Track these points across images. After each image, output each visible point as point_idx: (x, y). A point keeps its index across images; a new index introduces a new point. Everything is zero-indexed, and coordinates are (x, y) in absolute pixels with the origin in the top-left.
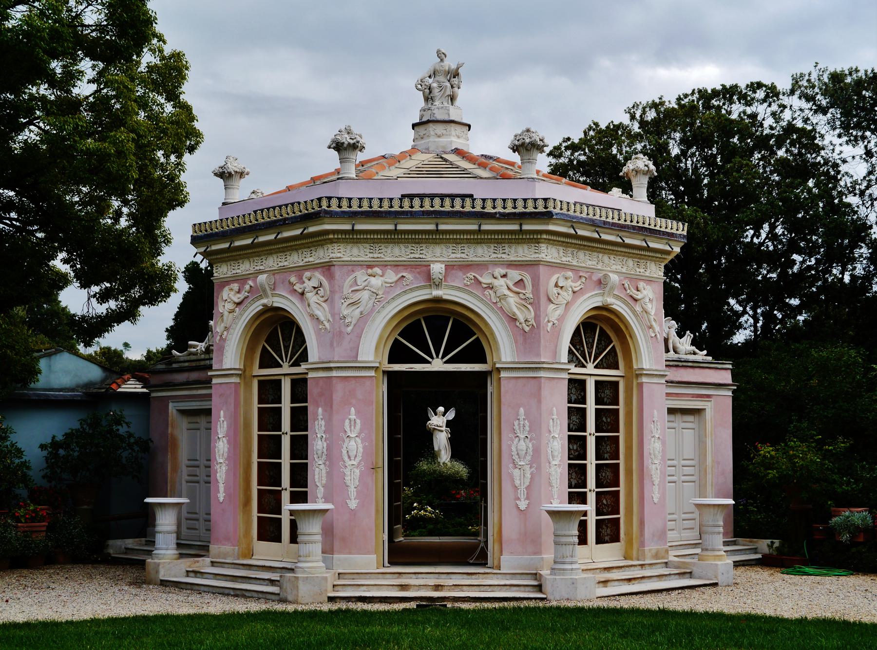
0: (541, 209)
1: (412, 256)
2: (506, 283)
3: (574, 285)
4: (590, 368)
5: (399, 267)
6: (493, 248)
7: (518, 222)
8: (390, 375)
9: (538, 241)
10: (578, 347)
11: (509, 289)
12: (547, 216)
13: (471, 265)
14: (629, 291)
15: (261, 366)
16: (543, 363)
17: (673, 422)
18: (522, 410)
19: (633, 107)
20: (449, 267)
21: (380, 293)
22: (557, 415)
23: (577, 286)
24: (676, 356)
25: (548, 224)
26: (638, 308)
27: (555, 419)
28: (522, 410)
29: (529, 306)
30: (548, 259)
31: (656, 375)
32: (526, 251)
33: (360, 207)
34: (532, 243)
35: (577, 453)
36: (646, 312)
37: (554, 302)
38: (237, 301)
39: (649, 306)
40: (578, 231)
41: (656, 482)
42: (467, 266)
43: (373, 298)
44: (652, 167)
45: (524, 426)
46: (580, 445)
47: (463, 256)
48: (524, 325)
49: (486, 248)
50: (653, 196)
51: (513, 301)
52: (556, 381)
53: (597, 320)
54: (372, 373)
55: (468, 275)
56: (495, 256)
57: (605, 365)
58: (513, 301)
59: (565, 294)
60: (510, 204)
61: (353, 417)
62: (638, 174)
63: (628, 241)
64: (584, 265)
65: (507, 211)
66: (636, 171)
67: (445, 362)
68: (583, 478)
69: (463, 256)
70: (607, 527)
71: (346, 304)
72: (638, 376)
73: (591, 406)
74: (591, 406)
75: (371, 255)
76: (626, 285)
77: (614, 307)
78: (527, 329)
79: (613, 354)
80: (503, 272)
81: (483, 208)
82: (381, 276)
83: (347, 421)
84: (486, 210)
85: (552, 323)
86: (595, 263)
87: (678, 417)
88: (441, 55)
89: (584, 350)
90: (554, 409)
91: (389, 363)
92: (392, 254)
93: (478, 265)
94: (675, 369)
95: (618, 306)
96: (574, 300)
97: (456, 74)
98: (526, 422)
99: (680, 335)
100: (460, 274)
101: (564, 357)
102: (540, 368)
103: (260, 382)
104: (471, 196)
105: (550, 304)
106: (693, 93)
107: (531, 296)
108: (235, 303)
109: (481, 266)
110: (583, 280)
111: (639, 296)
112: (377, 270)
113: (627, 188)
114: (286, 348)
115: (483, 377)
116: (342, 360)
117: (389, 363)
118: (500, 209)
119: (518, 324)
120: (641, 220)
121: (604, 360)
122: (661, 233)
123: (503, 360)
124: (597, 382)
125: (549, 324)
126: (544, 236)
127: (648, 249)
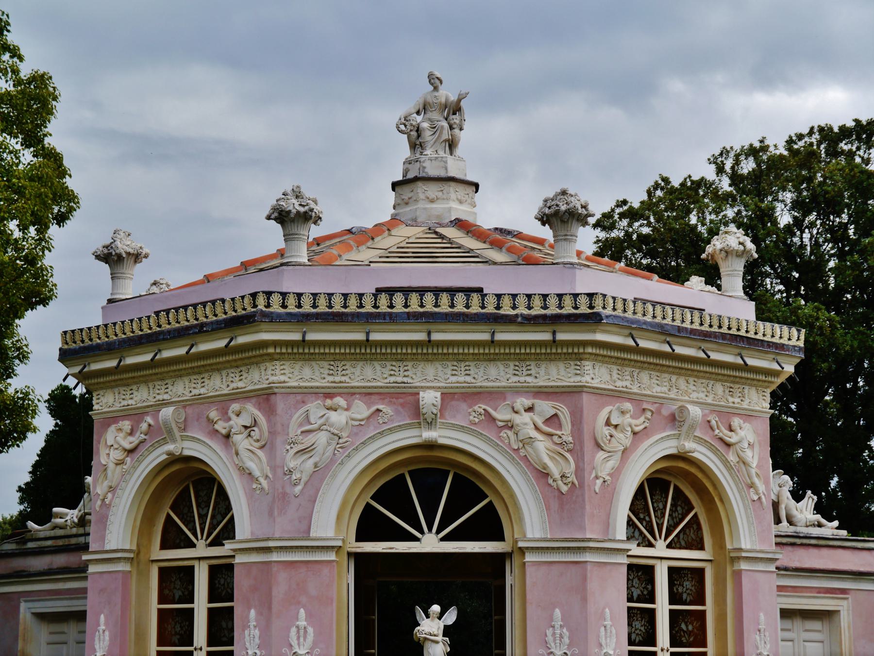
0: (584, 309)
1: (392, 379)
2: (532, 420)
3: (634, 422)
4: (660, 548)
5: (373, 397)
6: (512, 367)
7: (551, 328)
8: (359, 559)
9: (579, 357)
10: (642, 516)
11: (537, 428)
12: (594, 319)
13: (480, 393)
14: (717, 431)
15: (164, 546)
16: (590, 540)
17: (789, 630)
18: (558, 613)
19: (721, 154)
20: (448, 396)
21: (344, 434)
22: (611, 620)
23: (639, 423)
24: (791, 530)
25: (594, 332)
26: (732, 458)
27: (608, 627)
28: (558, 613)
29: (568, 455)
30: (595, 383)
32: (562, 372)
33: (314, 306)
34: (571, 359)
36: (744, 463)
37: (605, 448)
38: (128, 446)
39: (748, 455)
40: (639, 341)
42: (473, 395)
43: (334, 443)
44: (750, 246)
45: (561, 637)
47: (468, 379)
48: (560, 482)
49: (502, 368)
50: (752, 289)
51: (542, 447)
52: (609, 567)
53: (670, 474)
54: (332, 556)
55: (476, 408)
56: (516, 379)
57: (683, 543)
58: (542, 447)
59: (621, 435)
60: (537, 302)
61: (302, 623)
62: (730, 257)
63: (714, 356)
64: (649, 393)
65: (533, 312)
66: (726, 252)
67: (442, 539)
69: (468, 379)
71: (292, 452)
72: (734, 560)
73: (663, 607)
74: (663, 607)
75: (331, 378)
76: (713, 423)
77: (695, 455)
78: (564, 489)
79: (695, 527)
80: (528, 403)
81: (498, 307)
82: (347, 410)
83: (293, 630)
84: (502, 312)
85: (601, 480)
86: (665, 389)
87: (798, 624)
88: (435, 81)
89: (651, 521)
90: (607, 610)
91: (357, 540)
92: (486, 377)
93: (490, 393)
94: (790, 548)
95: (702, 454)
96: (634, 445)
97: (456, 109)
98: (565, 630)
99: (798, 496)
100: (464, 406)
101: (621, 532)
102: (584, 548)
103: (162, 570)
104: (480, 290)
105: (598, 452)
106: (811, 132)
107: (570, 439)
108: (125, 450)
109: (495, 395)
110: (649, 414)
111: (733, 438)
112: (340, 401)
113: (712, 276)
114: (203, 518)
115: (498, 562)
116: (286, 536)
117: (357, 540)
118: (522, 310)
119: (550, 481)
120: (734, 325)
121: (681, 536)
122: (766, 344)
123: (529, 535)
124: (671, 570)
125: (598, 481)
126: (589, 350)
127: (746, 367)
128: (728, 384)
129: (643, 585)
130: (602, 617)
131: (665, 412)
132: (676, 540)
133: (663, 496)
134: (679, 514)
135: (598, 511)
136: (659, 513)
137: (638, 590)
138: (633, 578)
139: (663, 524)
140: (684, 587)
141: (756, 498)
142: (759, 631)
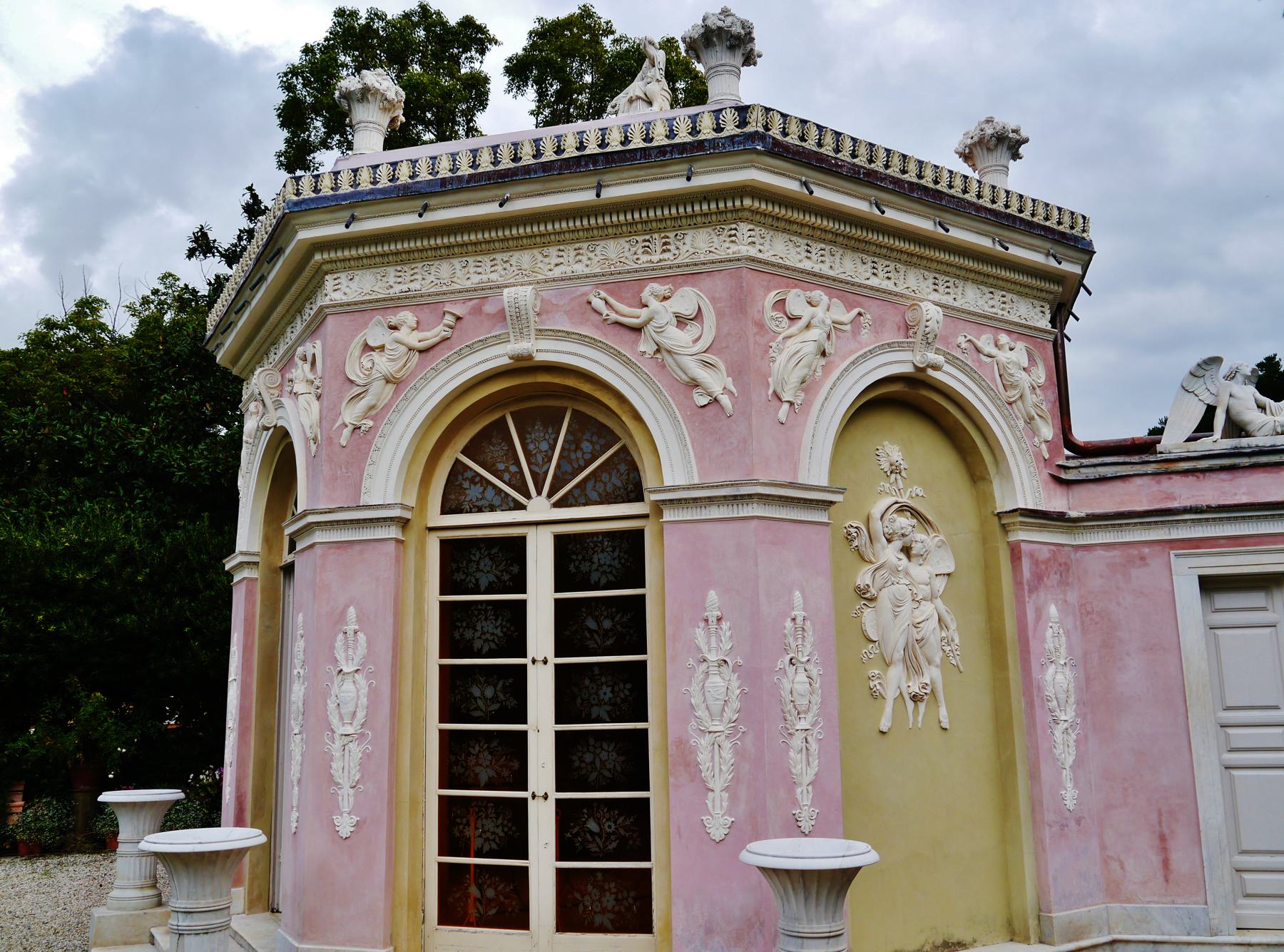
4: (539, 507)
10: (501, 466)
17: (1264, 609)
27: (350, 633)
30: (352, 297)
31: (711, 500)
35: (495, 707)
39: (677, 338)
41: (718, 784)
46: (504, 686)
52: (358, 548)
57: (594, 496)
68: (516, 765)
70: (603, 891)
85: (350, 428)
90: (352, 610)
94: (1223, 476)
110: (449, 319)
124: (560, 540)
128: (640, 239)
129: (502, 567)
130: (342, 618)
131: (489, 308)
132: (577, 492)
133: (550, 431)
134: (584, 453)
135: (344, 471)
136: (539, 458)
137: (489, 575)
138: (480, 558)
139: (546, 473)
140: (593, 563)
141: (704, 401)
142: (706, 621)
